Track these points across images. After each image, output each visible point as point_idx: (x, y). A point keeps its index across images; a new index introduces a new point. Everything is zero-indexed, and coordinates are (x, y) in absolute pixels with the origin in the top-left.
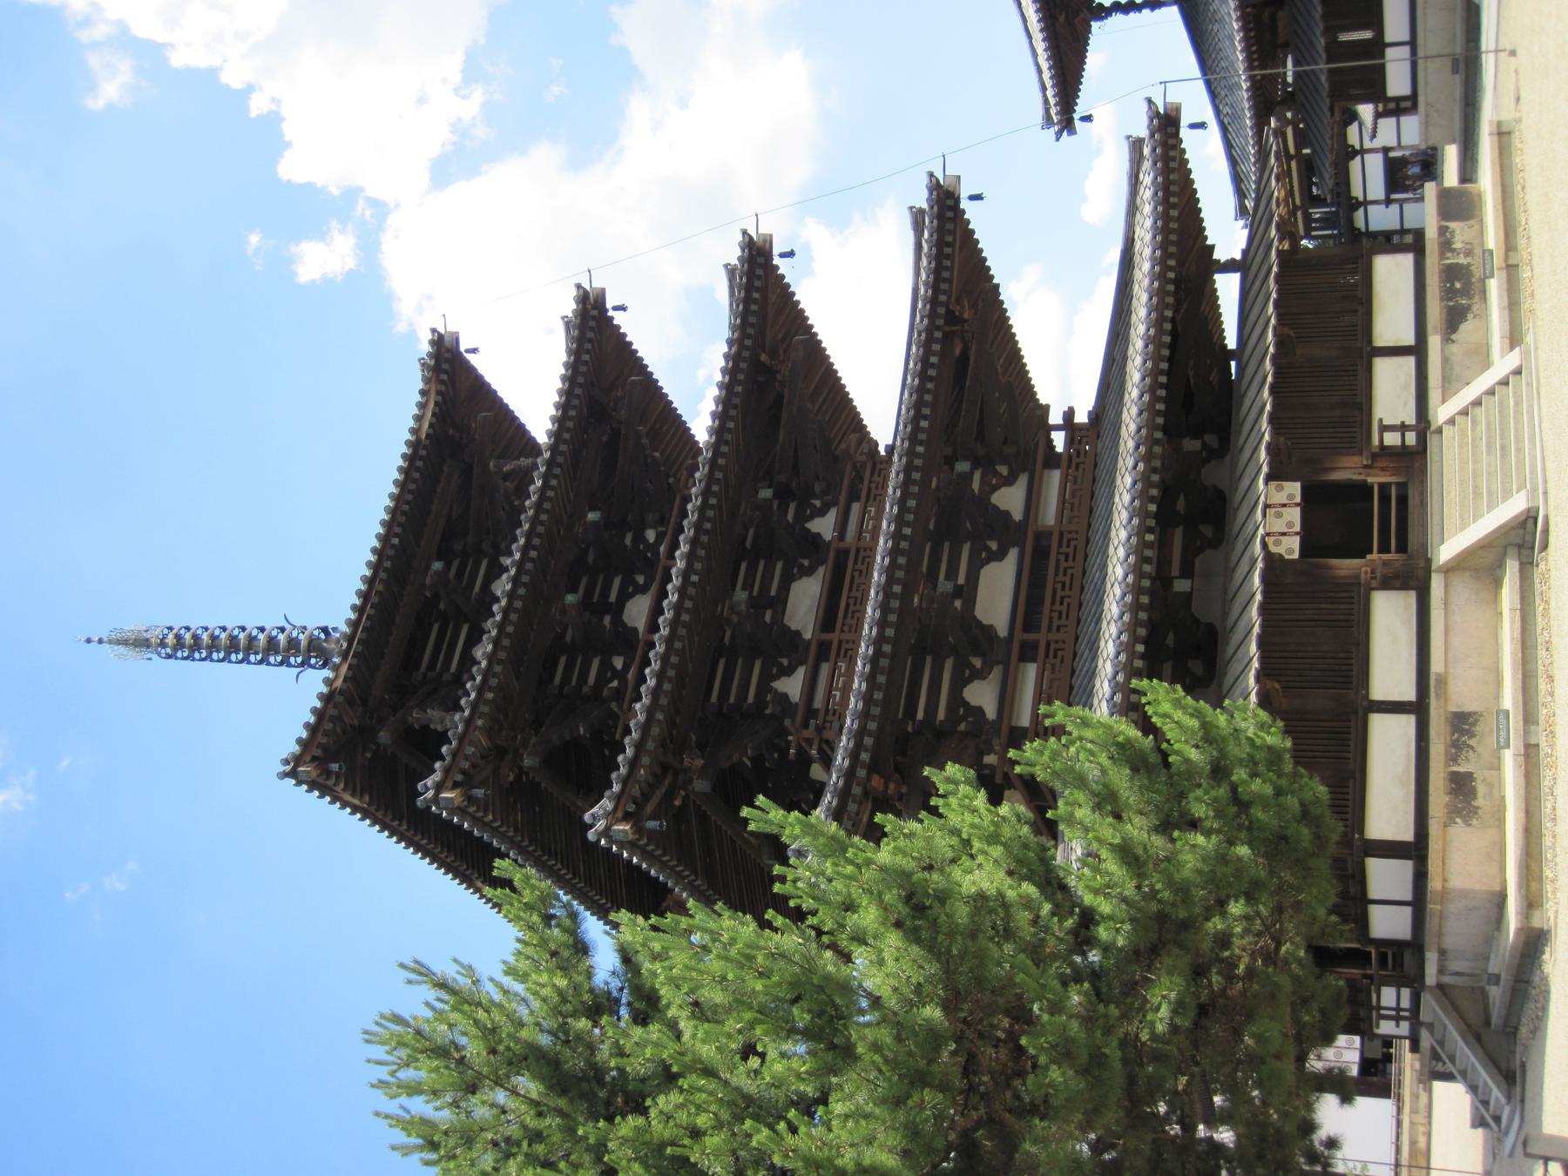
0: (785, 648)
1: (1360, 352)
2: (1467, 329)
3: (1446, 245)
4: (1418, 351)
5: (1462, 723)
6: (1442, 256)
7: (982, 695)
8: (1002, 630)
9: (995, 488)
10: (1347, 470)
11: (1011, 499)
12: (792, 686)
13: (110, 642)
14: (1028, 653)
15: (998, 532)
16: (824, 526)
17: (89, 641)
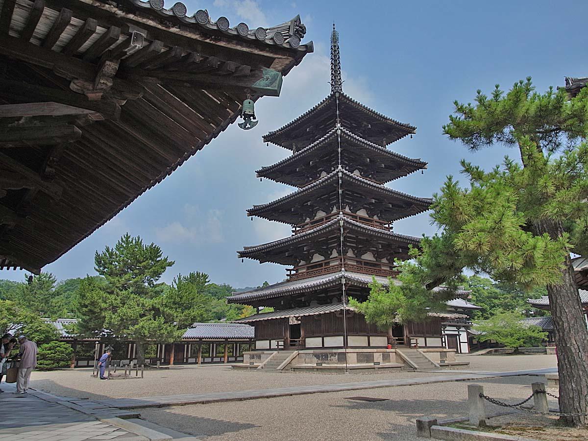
0: (312, 214)
1: (323, 334)
2: (315, 359)
3: (333, 354)
4: (323, 347)
5: (259, 357)
6: (330, 353)
7: (302, 263)
8: (311, 262)
9: (336, 249)
10: (302, 333)
11: (335, 254)
12: (308, 220)
13: (334, 31)
14: (308, 268)
15: (326, 254)
16: (335, 211)
17: (334, 25)
